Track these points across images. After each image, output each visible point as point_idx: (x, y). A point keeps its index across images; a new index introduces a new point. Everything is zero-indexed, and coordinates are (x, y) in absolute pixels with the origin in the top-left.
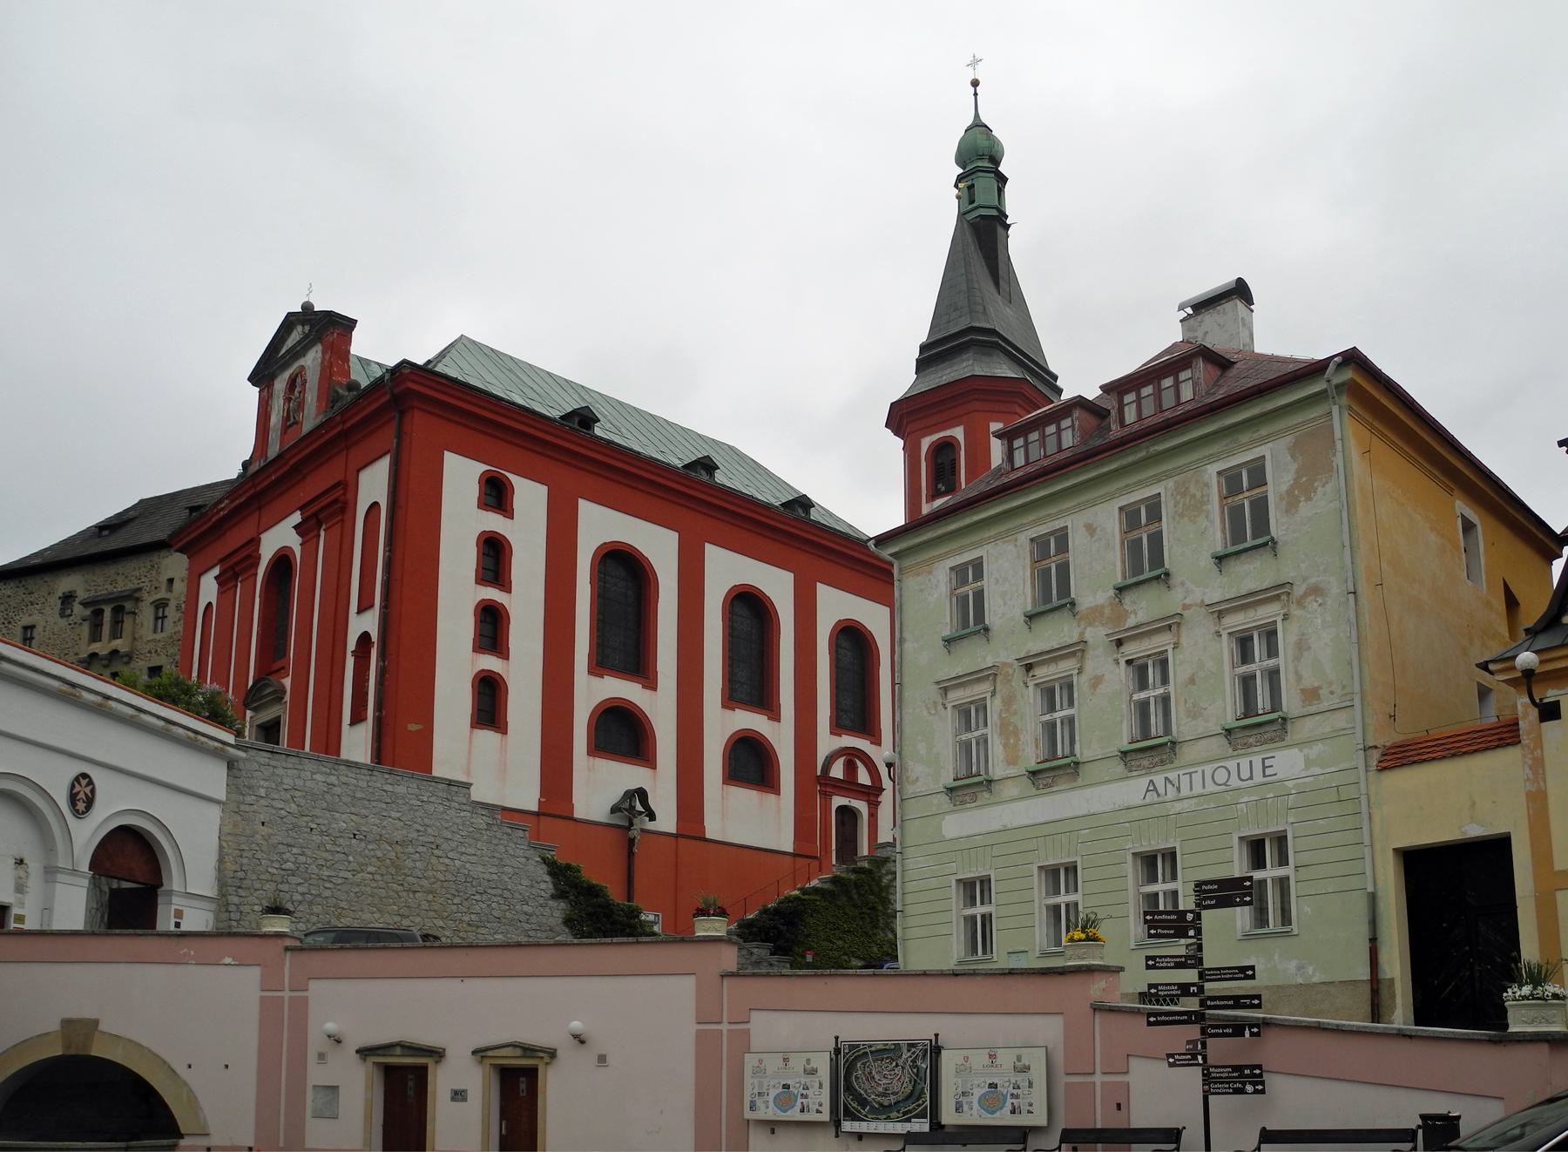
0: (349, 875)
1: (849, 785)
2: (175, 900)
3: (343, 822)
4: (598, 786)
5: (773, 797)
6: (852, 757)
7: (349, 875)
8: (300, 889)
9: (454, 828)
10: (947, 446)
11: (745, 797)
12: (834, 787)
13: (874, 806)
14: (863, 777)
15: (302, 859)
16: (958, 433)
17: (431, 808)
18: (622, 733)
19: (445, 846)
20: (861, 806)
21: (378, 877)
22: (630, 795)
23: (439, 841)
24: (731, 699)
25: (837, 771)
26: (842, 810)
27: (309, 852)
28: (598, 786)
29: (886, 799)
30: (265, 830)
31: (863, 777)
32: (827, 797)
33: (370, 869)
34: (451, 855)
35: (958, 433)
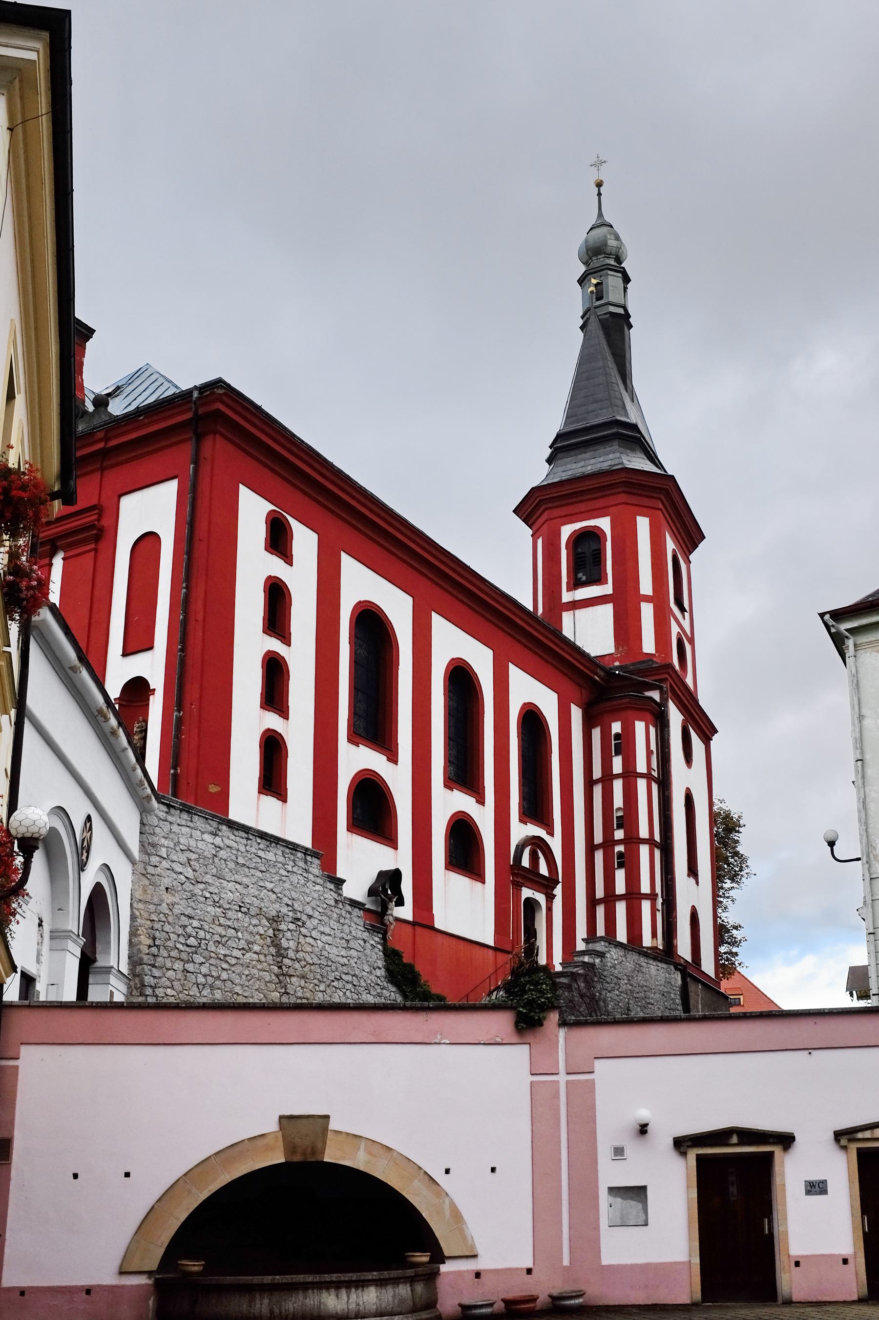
0: (238, 953)
1: (532, 877)
2: (113, 980)
3: (230, 893)
4: (361, 861)
5: (480, 884)
6: (537, 845)
7: (238, 953)
8: (204, 970)
9: (313, 904)
10: (592, 536)
11: (460, 882)
12: (524, 878)
13: (550, 898)
14: (544, 870)
15: (201, 934)
16: (604, 524)
17: (294, 878)
18: (372, 809)
19: (309, 924)
20: (541, 898)
21: (262, 957)
22: (381, 874)
23: (304, 918)
24: (450, 783)
25: (526, 862)
26: (528, 900)
27: (206, 927)
28: (361, 861)
29: (558, 891)
30: (168, 898)
31: (544, 870)
32: (518, 887)
33: (256, 948)
34: (315, 934)
35: (604, 524)
